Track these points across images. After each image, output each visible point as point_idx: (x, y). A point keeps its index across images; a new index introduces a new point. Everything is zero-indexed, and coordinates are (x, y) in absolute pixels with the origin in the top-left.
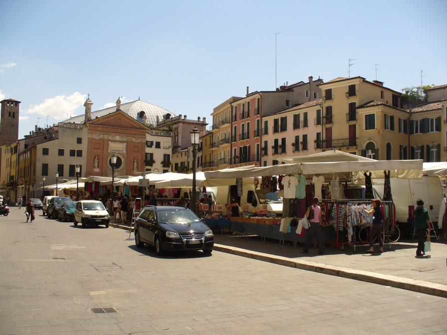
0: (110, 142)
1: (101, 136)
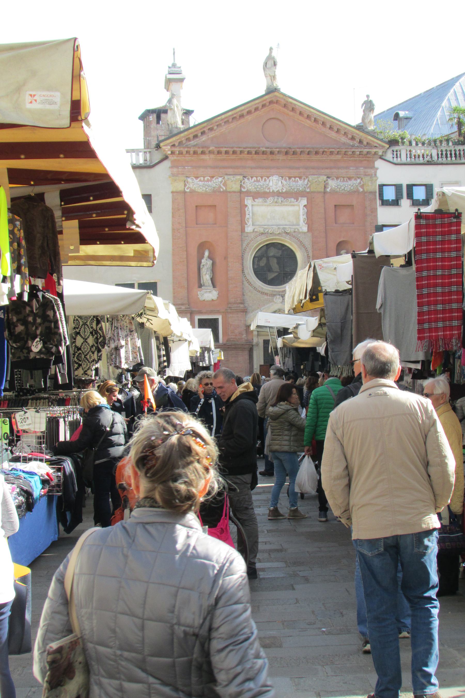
0: (248, 201)
1: (217, 182)
